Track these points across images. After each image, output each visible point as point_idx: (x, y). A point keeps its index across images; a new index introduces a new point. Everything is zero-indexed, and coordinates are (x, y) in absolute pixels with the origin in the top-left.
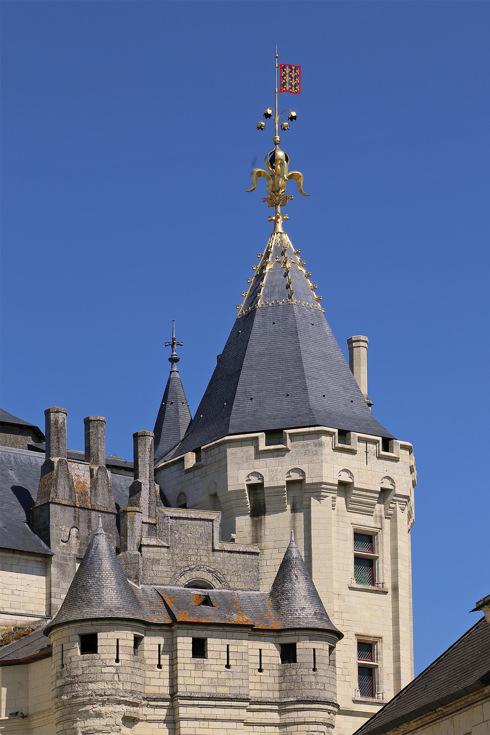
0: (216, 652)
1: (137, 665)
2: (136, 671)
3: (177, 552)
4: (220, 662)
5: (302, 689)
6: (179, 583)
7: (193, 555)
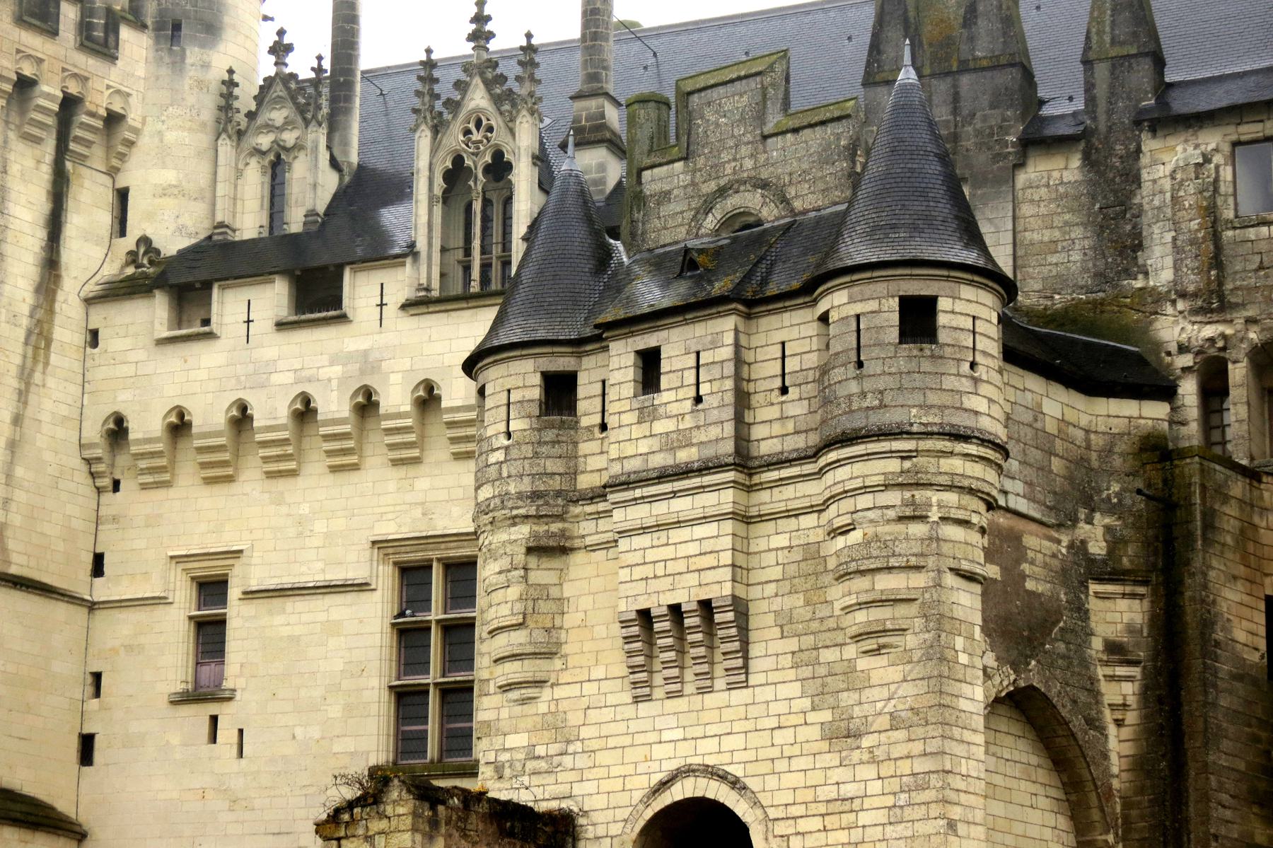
1: (550, 435)
2: (544, 449)
3: (701, 162)
4: (681, 394)
7: (729, 161)
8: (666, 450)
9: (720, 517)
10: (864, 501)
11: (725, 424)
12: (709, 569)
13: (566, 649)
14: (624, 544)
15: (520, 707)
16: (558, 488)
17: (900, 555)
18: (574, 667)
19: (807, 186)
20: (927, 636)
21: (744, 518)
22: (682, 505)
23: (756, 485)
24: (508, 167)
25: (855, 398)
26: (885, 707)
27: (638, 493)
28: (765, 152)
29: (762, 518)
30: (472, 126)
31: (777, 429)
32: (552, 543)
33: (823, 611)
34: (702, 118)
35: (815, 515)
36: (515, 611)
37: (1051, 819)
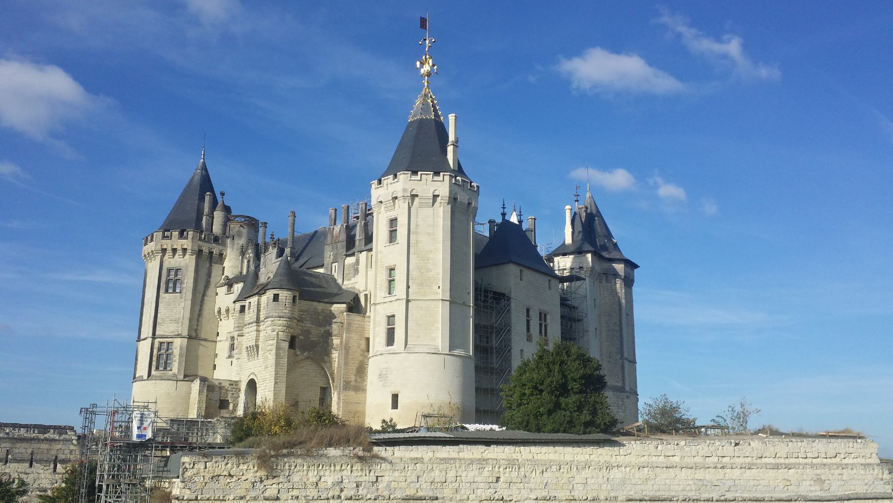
1: (241, 317)
21: (258, 331)
22: (251, 329)
37: (321, 379)
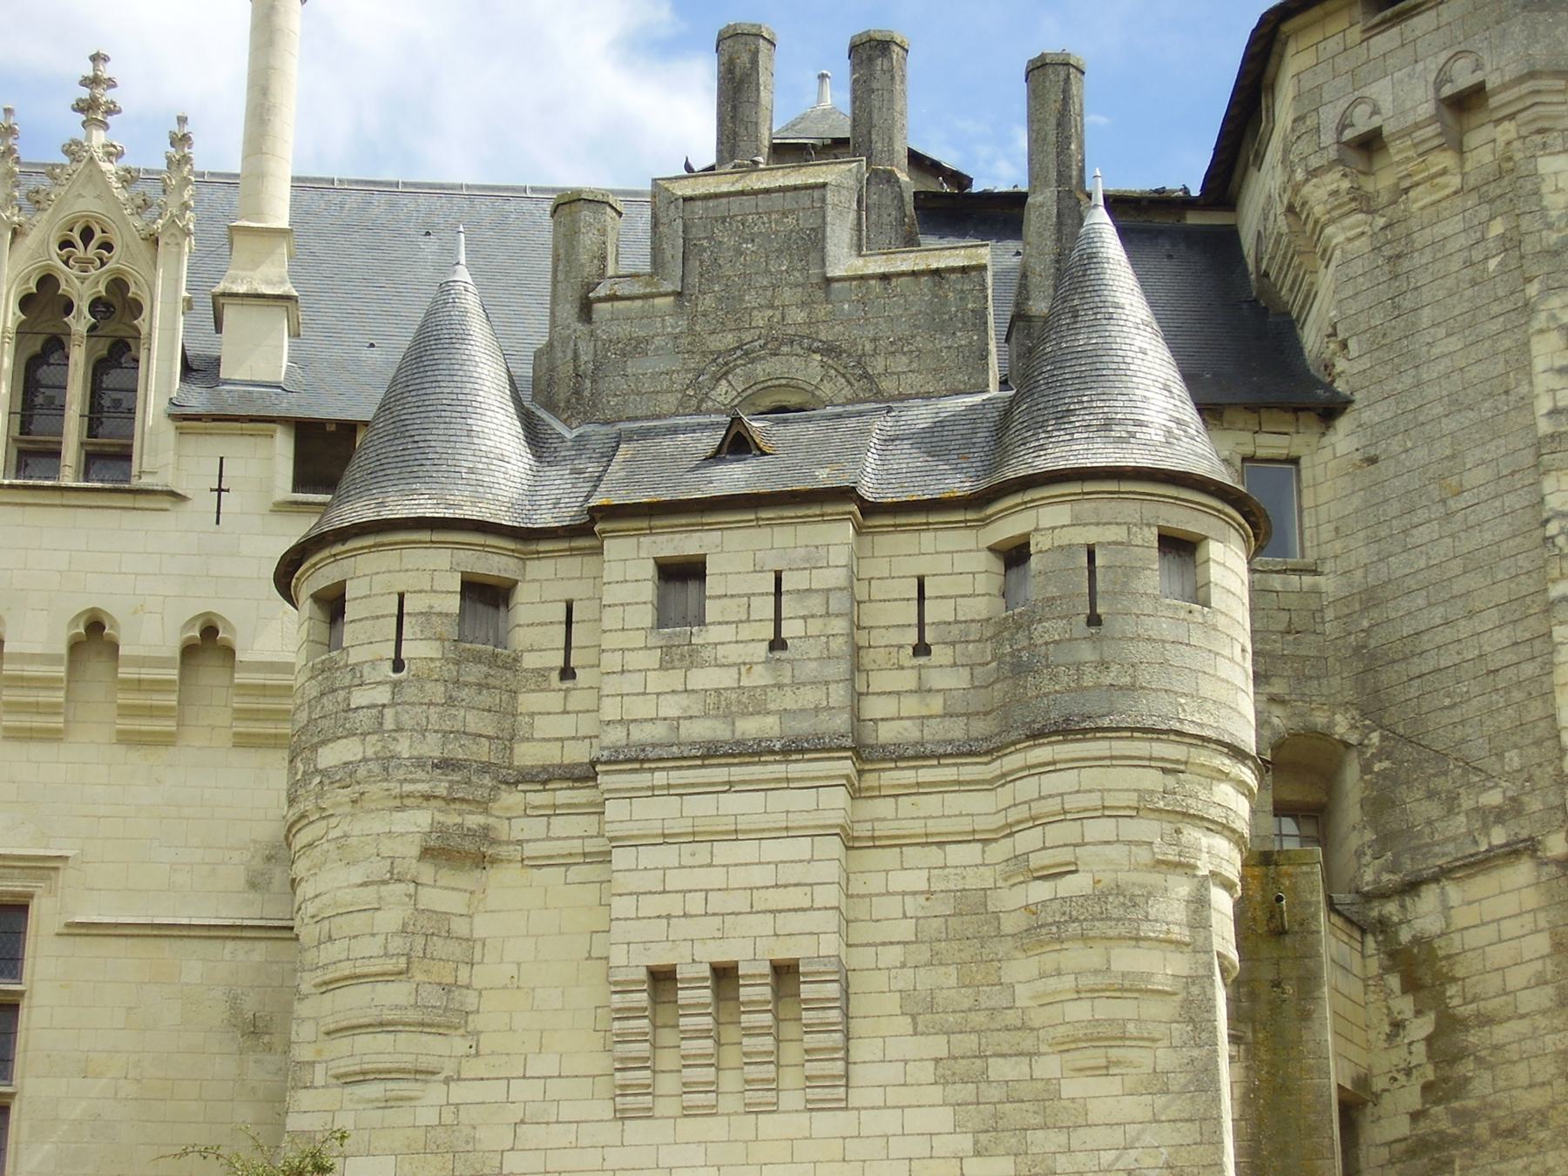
0: (736, 600)
1: (474, 672)
4: (746, 632)
5: (1046, 695)
6: (710, 403)
8: (716, 717)
9: (817, 833)
10: (1099, 829)
11: (832, 687)
12: (795, 910)
13: (475, 1022)
14: (621, 858)
15: (380, 1111)
16: (485, 759)
17: (1156, 921)
18: (493, 1053)
19: (905, 360)
20: (1196, 1053)
23: (867, 789)
24: (136, 308)
25: (1088, 669)
26: (1117, 1159)
27: (660, 778)
28: (827, 301)
29: (875, 842)
30: (76, 236)
31: (911, 706)
32: (468, 845)
33: (998, 999)
34: (710, 238)
35: (979, 846)
36: (391, 951)
